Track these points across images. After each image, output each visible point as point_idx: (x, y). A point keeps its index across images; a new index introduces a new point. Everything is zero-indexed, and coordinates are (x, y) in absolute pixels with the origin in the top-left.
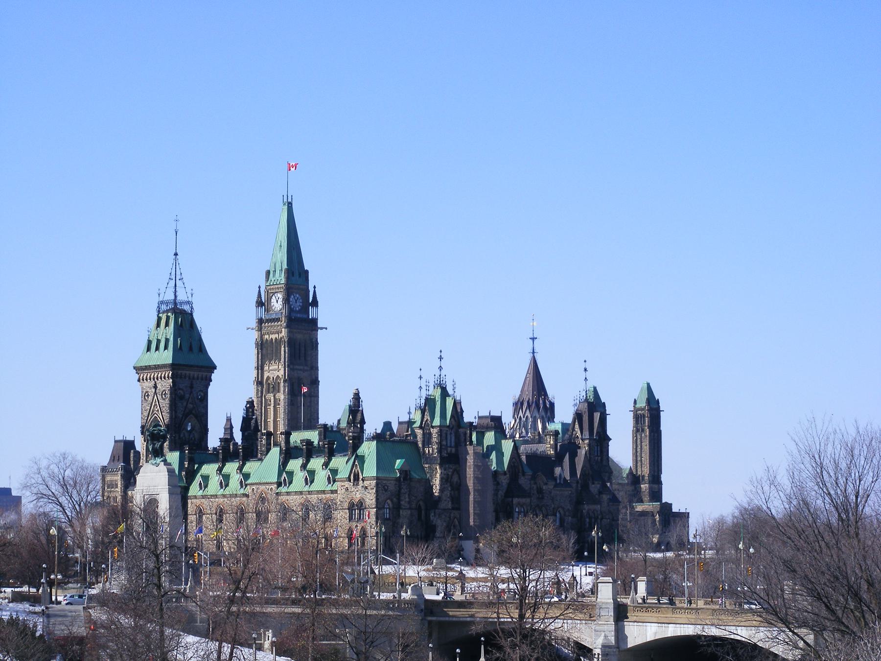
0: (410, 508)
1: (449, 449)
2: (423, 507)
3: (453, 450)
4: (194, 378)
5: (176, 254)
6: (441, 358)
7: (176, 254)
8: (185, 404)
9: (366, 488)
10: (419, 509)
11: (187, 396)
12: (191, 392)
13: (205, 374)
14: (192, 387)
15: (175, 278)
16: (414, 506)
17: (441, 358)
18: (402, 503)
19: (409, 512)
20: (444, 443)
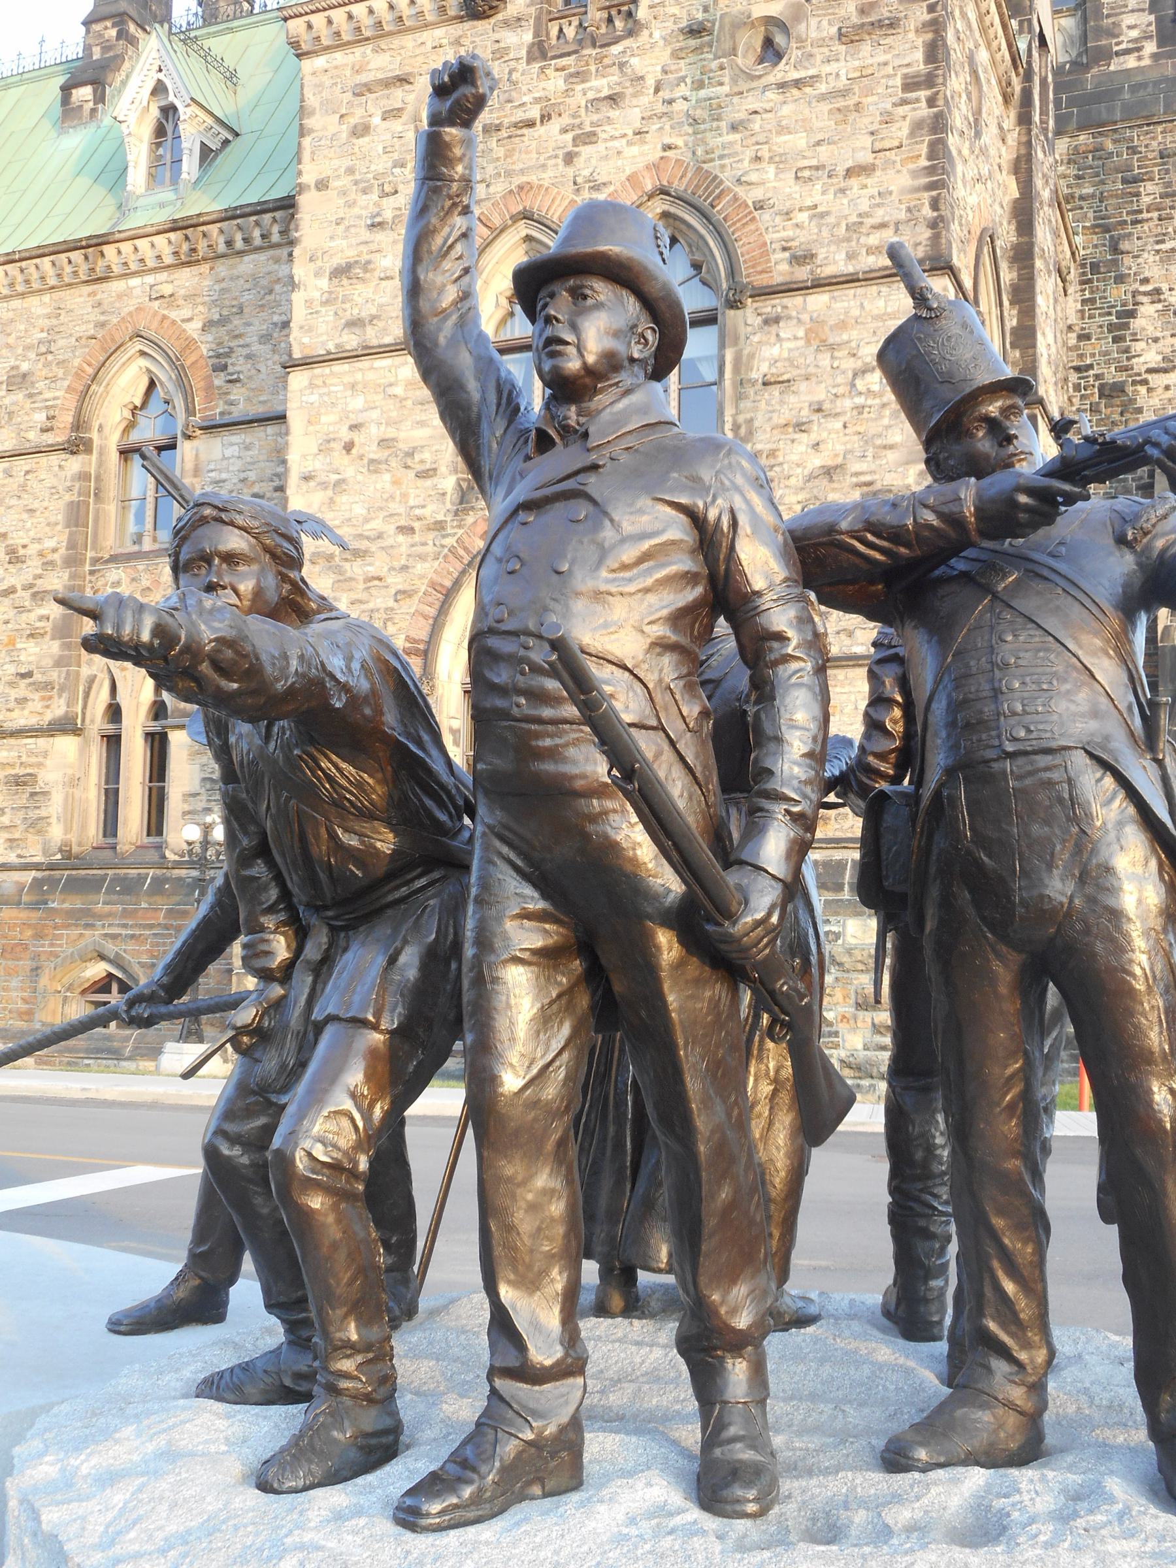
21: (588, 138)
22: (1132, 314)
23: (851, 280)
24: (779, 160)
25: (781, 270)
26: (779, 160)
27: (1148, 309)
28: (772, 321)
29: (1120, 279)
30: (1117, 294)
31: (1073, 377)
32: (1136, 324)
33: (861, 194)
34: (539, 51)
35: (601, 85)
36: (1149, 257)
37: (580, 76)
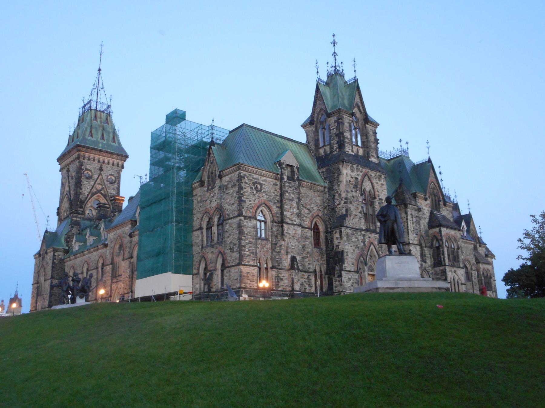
0: (300, 225)
1: (355, 148)
2: (321, 228)
3: (361, 152)
4: (104, 162)
5: (100, 70)
6: (334, 43)
7: (100, 70)
8: (92, 183)
9: (226, 187)
10: (316, 230)
11: (95, 177)
12: (100, 174)
13: (116, 161)
14: (101, 169)
15: (98, 88)
16: (307, 223)
17: (334, 43)
18: (287, 214)
19: (299, 230)
20: (347, 134)
21: (211, 202)
22: (335, 196)
23: (232, 218)
24: (227, 203)
25: (227, 217)
26: (227, 203)
27: (337, 195)
28: (226, 224)
29: (333, 190)
30: (333, 192)
31: (328, 207)
32: (336, 197)
33: (234, 206)
34: (208, 191)
35: (212, 194)
36: (336, 186)
37: (211, 194)
